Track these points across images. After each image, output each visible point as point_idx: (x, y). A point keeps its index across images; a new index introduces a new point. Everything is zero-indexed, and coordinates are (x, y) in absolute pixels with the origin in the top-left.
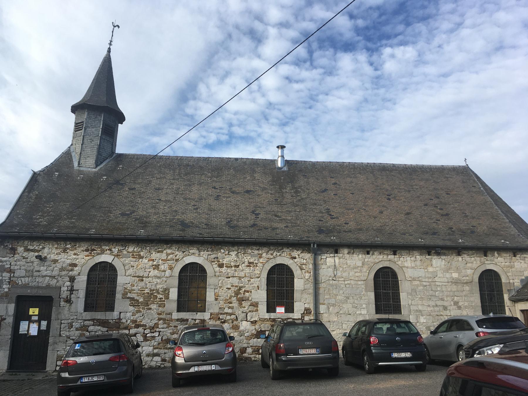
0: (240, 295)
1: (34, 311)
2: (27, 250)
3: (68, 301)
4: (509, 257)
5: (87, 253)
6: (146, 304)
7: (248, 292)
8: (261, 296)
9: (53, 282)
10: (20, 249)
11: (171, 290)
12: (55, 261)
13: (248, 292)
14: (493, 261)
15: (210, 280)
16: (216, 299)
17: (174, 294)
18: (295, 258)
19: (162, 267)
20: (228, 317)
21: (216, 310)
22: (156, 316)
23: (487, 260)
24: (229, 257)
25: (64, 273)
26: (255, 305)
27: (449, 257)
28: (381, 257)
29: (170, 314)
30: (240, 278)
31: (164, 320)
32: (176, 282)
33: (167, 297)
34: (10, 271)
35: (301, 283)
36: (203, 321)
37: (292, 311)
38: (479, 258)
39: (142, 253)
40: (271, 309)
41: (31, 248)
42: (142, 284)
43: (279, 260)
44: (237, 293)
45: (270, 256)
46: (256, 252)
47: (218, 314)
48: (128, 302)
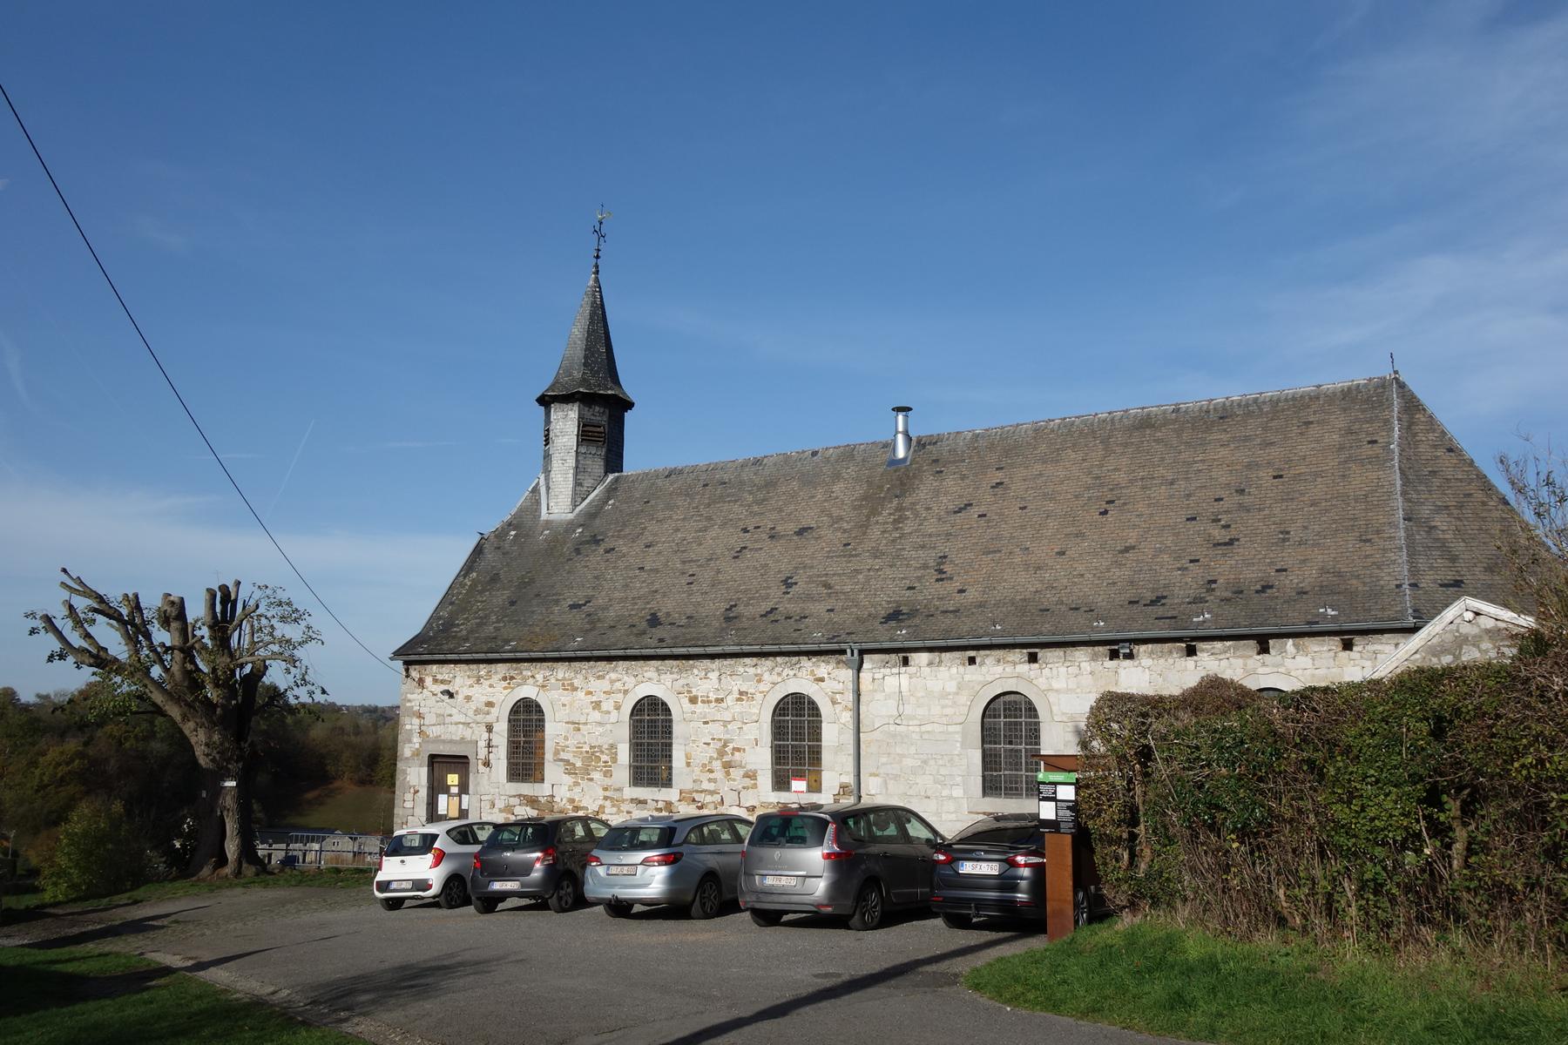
0: (727, 759)
1: (453, 779)
2: (435, 681)
3: (487, 764)
4: (1326, 655)
5: (505, 684)
6: (586, 771)
7: (738, 750)
8: (761, 758)
9: (468, 734)
10: (428, 681)
11: (620, 746)
12: (468, 698)
13: (738, 750)
14: (1278, 666)
15: (677, 729)
16: (688, 764)
17: (624, 754)
18: (822, 680)
19: (604, 706)
20: (709, 799)
21: (689, 786)
22: (601, 793)
23: (1264, 664)
24: (706, 679)
25: (479, 718)
26: (751, 775)
27: (1162, 661)
28: (999, 669)
29: (620, 790)
30: (725, 723)
31: (612, 799)
32: (624, 732)
33: (615, 760)
34: (420, 716)
35: (834, 733)
36: (669, 804)
37: (819, 790)
38: (1240, 662)
39: (576, 682)
40: (781, 783)
41: (439, 677)
42: (579, 737)
43: (793, 687)
44: (721, 753)
45: (775, 678)
46: (752, 671)
47: (691, 792)
48: (561, 767)
